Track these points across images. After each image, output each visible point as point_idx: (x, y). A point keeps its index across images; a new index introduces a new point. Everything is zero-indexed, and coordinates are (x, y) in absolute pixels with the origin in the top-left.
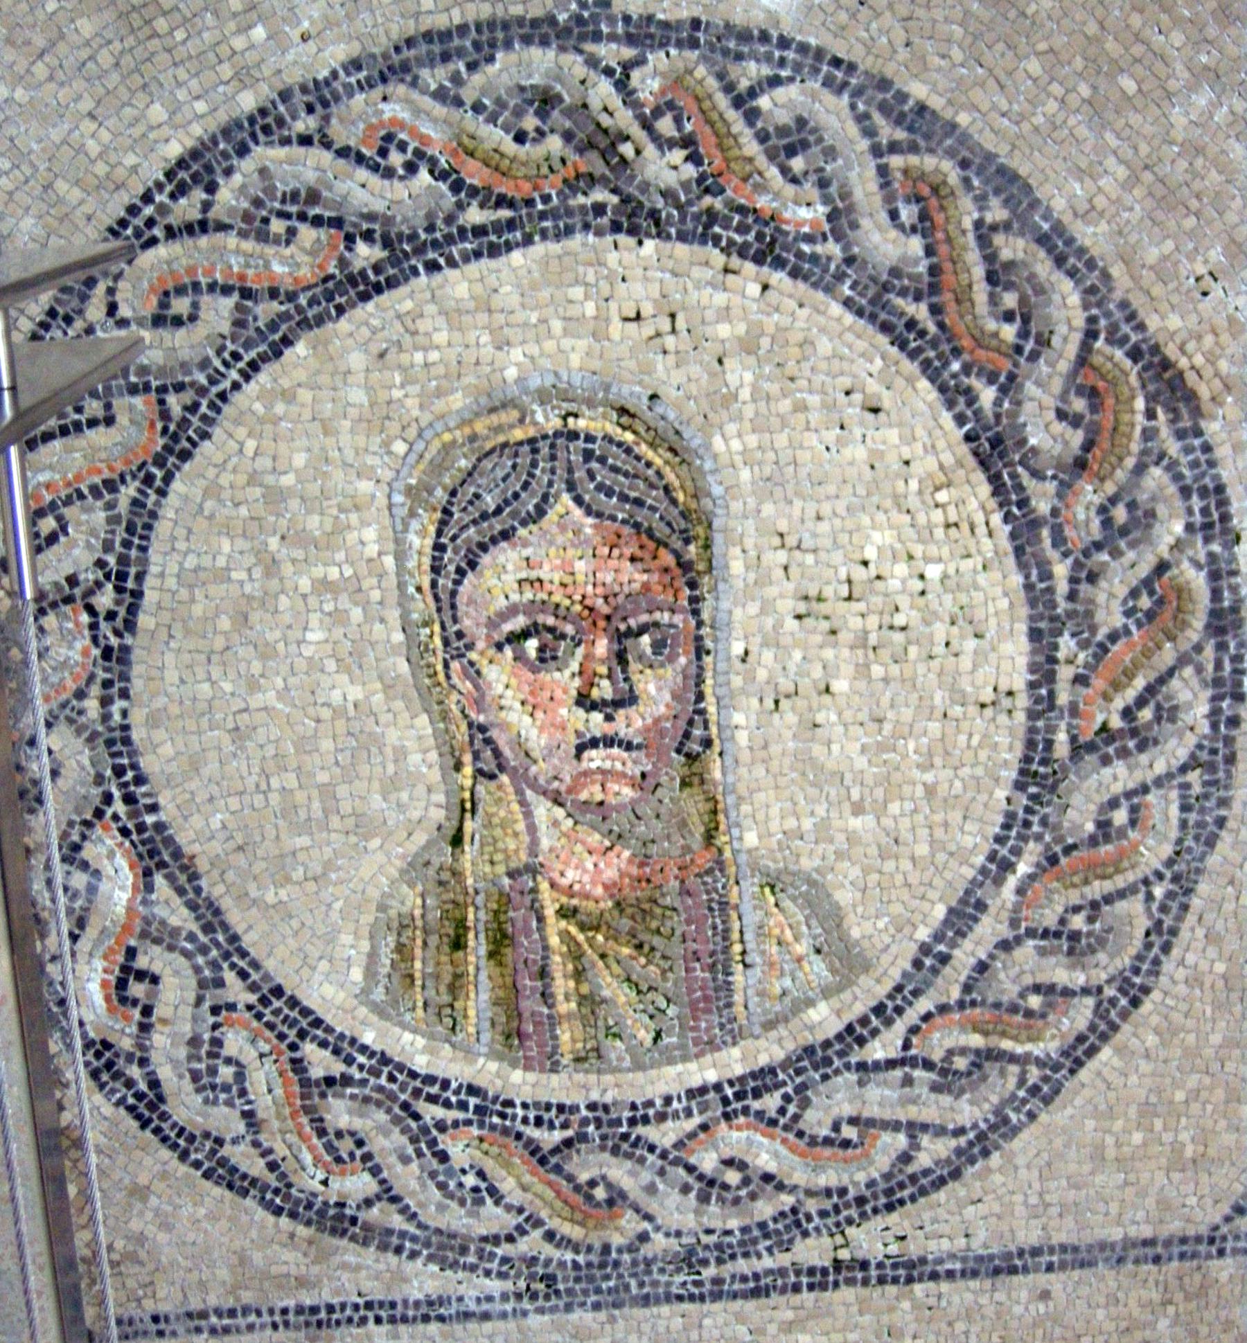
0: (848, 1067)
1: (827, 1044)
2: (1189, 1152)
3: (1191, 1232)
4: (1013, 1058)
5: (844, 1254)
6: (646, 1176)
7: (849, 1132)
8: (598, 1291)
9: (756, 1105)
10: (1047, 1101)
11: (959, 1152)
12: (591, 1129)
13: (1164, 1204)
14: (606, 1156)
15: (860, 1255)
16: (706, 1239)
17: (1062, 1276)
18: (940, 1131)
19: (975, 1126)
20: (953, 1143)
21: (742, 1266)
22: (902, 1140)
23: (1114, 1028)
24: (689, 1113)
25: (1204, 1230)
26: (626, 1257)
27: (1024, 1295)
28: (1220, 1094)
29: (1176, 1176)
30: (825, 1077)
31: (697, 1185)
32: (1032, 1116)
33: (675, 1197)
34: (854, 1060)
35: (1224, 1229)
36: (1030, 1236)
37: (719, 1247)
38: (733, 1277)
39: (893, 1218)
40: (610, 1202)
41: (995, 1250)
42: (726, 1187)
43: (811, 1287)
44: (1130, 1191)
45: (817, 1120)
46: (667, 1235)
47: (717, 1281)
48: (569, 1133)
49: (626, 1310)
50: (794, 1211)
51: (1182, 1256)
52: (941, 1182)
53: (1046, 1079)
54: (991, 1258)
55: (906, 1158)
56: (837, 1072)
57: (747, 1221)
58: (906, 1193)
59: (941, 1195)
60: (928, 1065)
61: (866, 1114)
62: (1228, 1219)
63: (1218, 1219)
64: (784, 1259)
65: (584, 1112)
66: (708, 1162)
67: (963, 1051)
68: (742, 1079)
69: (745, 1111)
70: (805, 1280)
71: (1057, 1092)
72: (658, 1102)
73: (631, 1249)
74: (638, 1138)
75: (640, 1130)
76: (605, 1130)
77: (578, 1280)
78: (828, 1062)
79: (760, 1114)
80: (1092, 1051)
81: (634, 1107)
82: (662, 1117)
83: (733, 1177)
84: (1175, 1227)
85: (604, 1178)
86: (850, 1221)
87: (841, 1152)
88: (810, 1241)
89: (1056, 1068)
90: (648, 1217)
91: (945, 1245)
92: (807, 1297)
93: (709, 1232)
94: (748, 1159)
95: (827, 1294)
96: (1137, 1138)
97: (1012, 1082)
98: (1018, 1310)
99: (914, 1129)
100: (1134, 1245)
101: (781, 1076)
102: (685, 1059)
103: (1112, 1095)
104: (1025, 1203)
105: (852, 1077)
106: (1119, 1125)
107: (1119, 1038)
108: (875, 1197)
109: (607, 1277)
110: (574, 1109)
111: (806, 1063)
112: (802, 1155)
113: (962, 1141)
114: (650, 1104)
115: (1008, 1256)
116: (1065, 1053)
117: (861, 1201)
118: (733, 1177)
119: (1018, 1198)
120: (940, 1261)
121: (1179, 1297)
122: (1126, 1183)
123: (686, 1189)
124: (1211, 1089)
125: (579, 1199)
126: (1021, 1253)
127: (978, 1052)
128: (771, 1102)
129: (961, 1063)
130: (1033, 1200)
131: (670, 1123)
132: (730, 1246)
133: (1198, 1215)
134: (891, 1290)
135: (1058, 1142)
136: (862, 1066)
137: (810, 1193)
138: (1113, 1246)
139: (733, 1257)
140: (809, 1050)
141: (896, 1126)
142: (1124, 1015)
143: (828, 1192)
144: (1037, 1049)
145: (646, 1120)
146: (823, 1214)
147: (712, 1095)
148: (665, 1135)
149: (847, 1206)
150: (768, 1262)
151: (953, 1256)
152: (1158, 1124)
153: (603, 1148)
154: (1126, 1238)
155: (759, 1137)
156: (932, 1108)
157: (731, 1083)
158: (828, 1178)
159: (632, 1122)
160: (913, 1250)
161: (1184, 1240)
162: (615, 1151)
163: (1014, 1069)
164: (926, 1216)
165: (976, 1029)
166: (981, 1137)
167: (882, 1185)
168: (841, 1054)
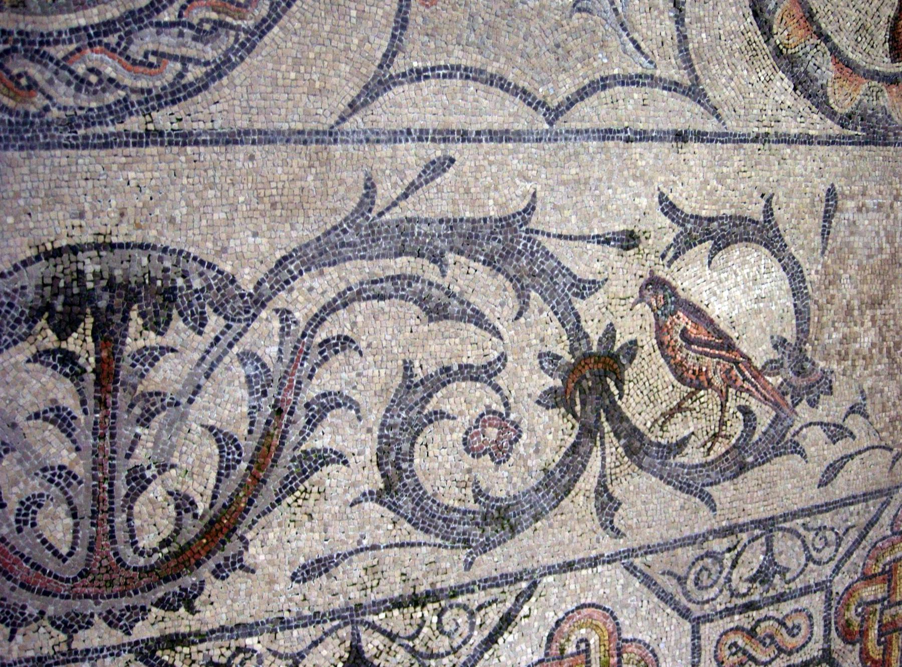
0: (151, 24)
1: (141, 10)
2: (317, 85)
3: (321, 128)
4: (232, 27)
5: (151, 127)
6: (48, 75)
7: (152, 59)
8: (22, 139)
9: (105, 40)
10: (249, 51)
11: (207, 74)
12: (19, 45)
13: (307, 113)
14: (27, 61)
15: (159, 127)
16: (79, 113)
17: (260, 148)
18: (198, 62)
19: (215, 61)
20: (204, 69)
21: (98, 129)
22: (178, 66)
23: (280, 17)
24: (71, 42)
25: (326, 128)
26: (37, 120)
27: (242, 156)
28: (330, 57)
29: (312, 98)
30: (140, 29)
31: (75, 82)
32: (242, 59)
33: (63, 88)
34: (154, 20)
35: (336, 128)
36: (243, 123)
37: (86, 117)
38: (94, 135)
39: (175, 108)
40: (29, 87)
41: (226, 130)
42: (90, 84)
43: (134, 144)
44: (290, 103)
45: (136, 50)
46: (59, 109)
47: (86, 137)
48: (8, 46)
49: (37, 151)
50: (125, 100)
51: (317, 141)
52: (198, 91)
53: (248, 40)
54: (224, 134)
55: (181, 75)
56: (146, 26)
57: (101, 104)
58: (181, 95)
59: (199, 98)
60: (191, 26)
61: (161, 50)
62: (338, 123)
63: (333, 123)
64: (120, 127)
65: (16, 36)
66: (81, 69)
67: (208, 21)
68: (98, 25)
69: (100, 43)
70: (131, 140)
71: (254, 46)
72: (55, 34)
73: (40, 115)
74: (45, 53)
75: (45, 48)
76: (27, 46)
77: (11, 131)
78: (141, 20)
79: (107, 45)
80: (270, 28)
81: (42, 35)
82: (57, 42)
83: (93, 79)
84: (312, 125)
85: (26, 73)
86: (154, 108)
87: (148, 70)
88: (134, 118)
89: (253, 34)
90: (49, 98)
91: (201, 125)
92: (132, 150)
93: (81, 108)
94: (101, 69)
95: (142, 150)
96: (293, 75)
97: (232, 39)
98: (239, 165)
99: (185, 60)
100: (294, 133)
101: (118, 26)
102: (69, 12)
103: (280, 51)
104: (240, 106)
105: (153, 30)
106: (284, 67)
107: (281, 22)
108: (166, 96)
109: (27, 131)
110: (10, 33)
111: (130, 20)
112: (129, 70)
113: (209, 68)
114: (50, 34)
115: (232, 134)
116: (257, 27)
117: (159, 97)
118: (93, 79)
119: (236, 102)
120: (199, 135)
121: (317, 164)
122: (289, 99)
123: (69, 83)
124: (326, 53)
125: (12, 85)
126: (239, 133)
127: (215, 22)
128: (113, 39)
129: (207, 27)
130: (244, 104)
131: (60, 46)
132: (92, 117)
133: (323, 120)
134: (175, 149)
135: (255, 74)
136: (158, 24)
137: (134, 91)
138: (283, 133)
139: (94, 124)
140: (132, 13)
141: (175, 58)
142: (284, 11)
143: (142, 91)
144: (244, 24)
145: (48, 43)
146: (140, 103)
147: (83, 33)
148: (58, 52)
149: (152, 99)
150: (111, 129)
151: (205, 132)
152: (302, 69)
153: (25, 56)
154: (290, 129)
155: (106, 58)
156: (193, 50)
157: (92, 27)
158: (142, 83)
159: (41, 43)
160: (186, 126)
161: (317, 132)
162: (32, 59)
163: (233, 33)
164: (192, 108)
165: (214, 10)
166: (218, 67)
167: (169, 90)
168: (149, 17)
